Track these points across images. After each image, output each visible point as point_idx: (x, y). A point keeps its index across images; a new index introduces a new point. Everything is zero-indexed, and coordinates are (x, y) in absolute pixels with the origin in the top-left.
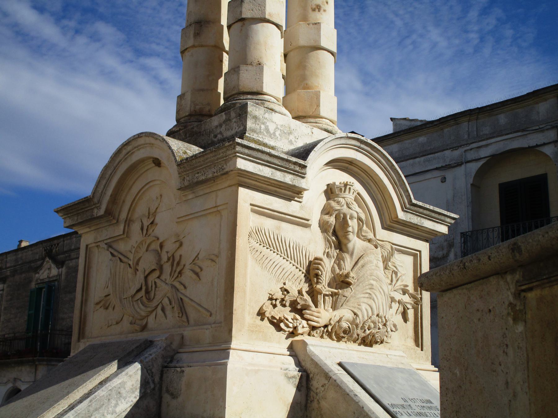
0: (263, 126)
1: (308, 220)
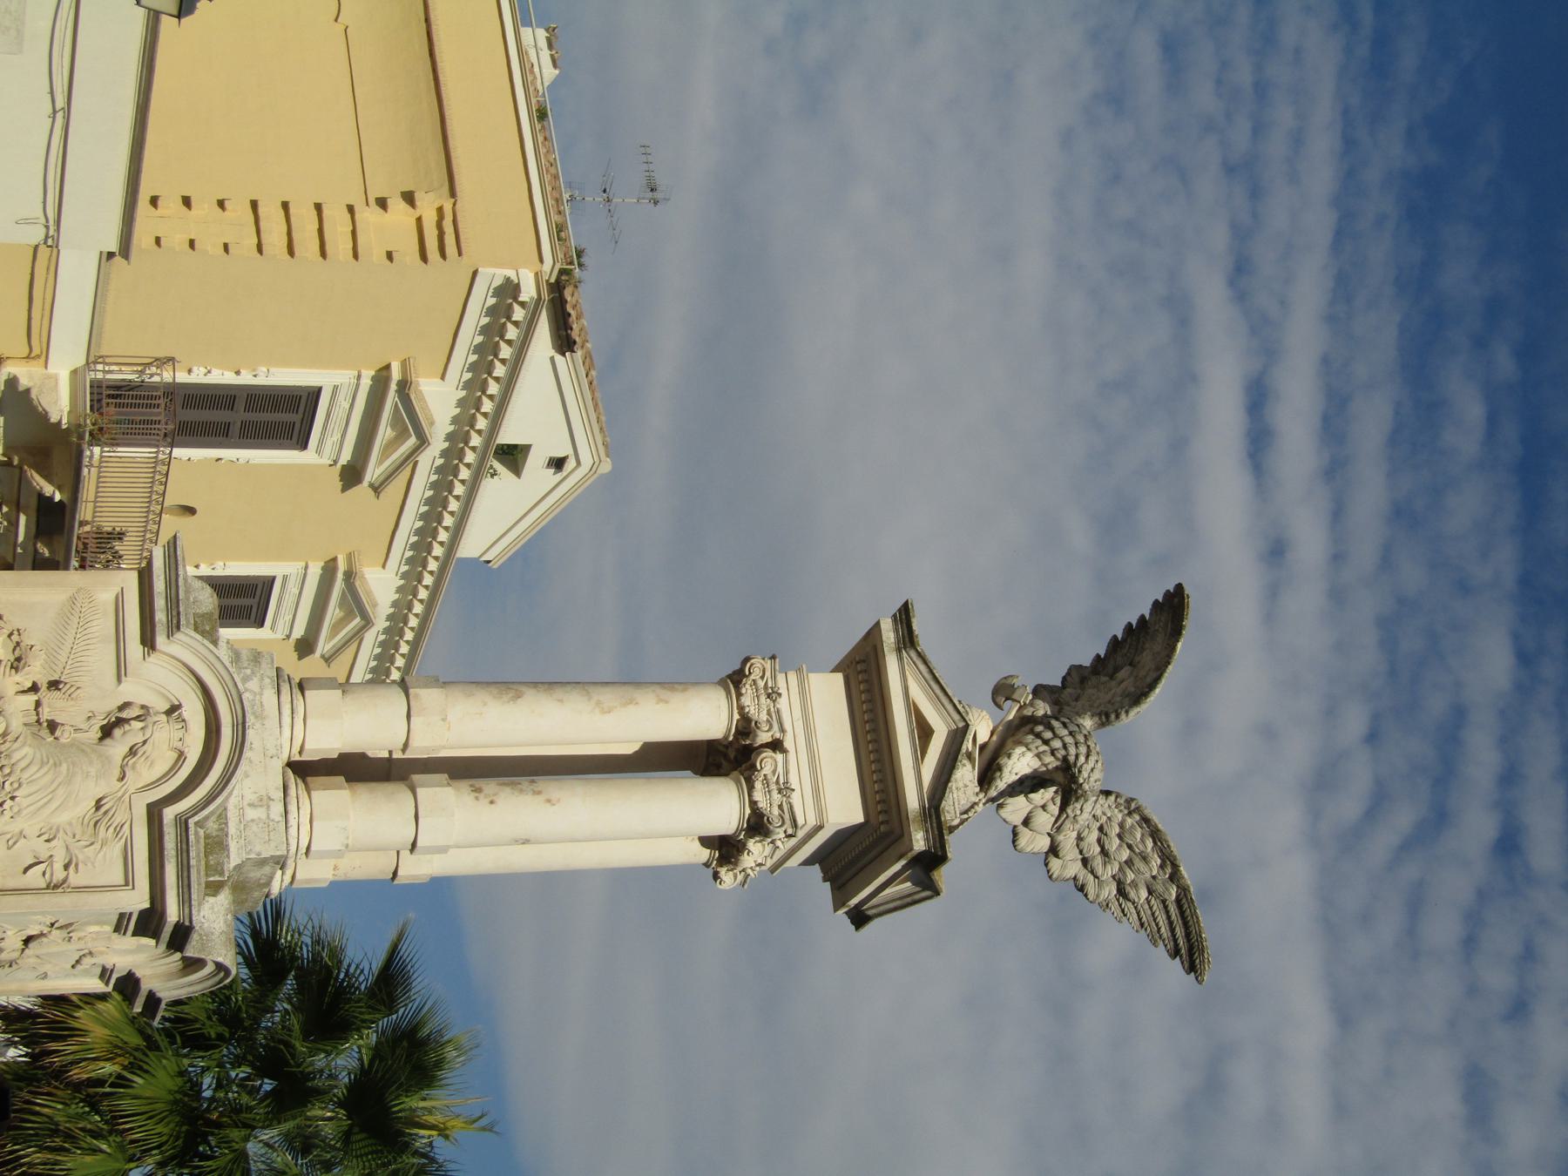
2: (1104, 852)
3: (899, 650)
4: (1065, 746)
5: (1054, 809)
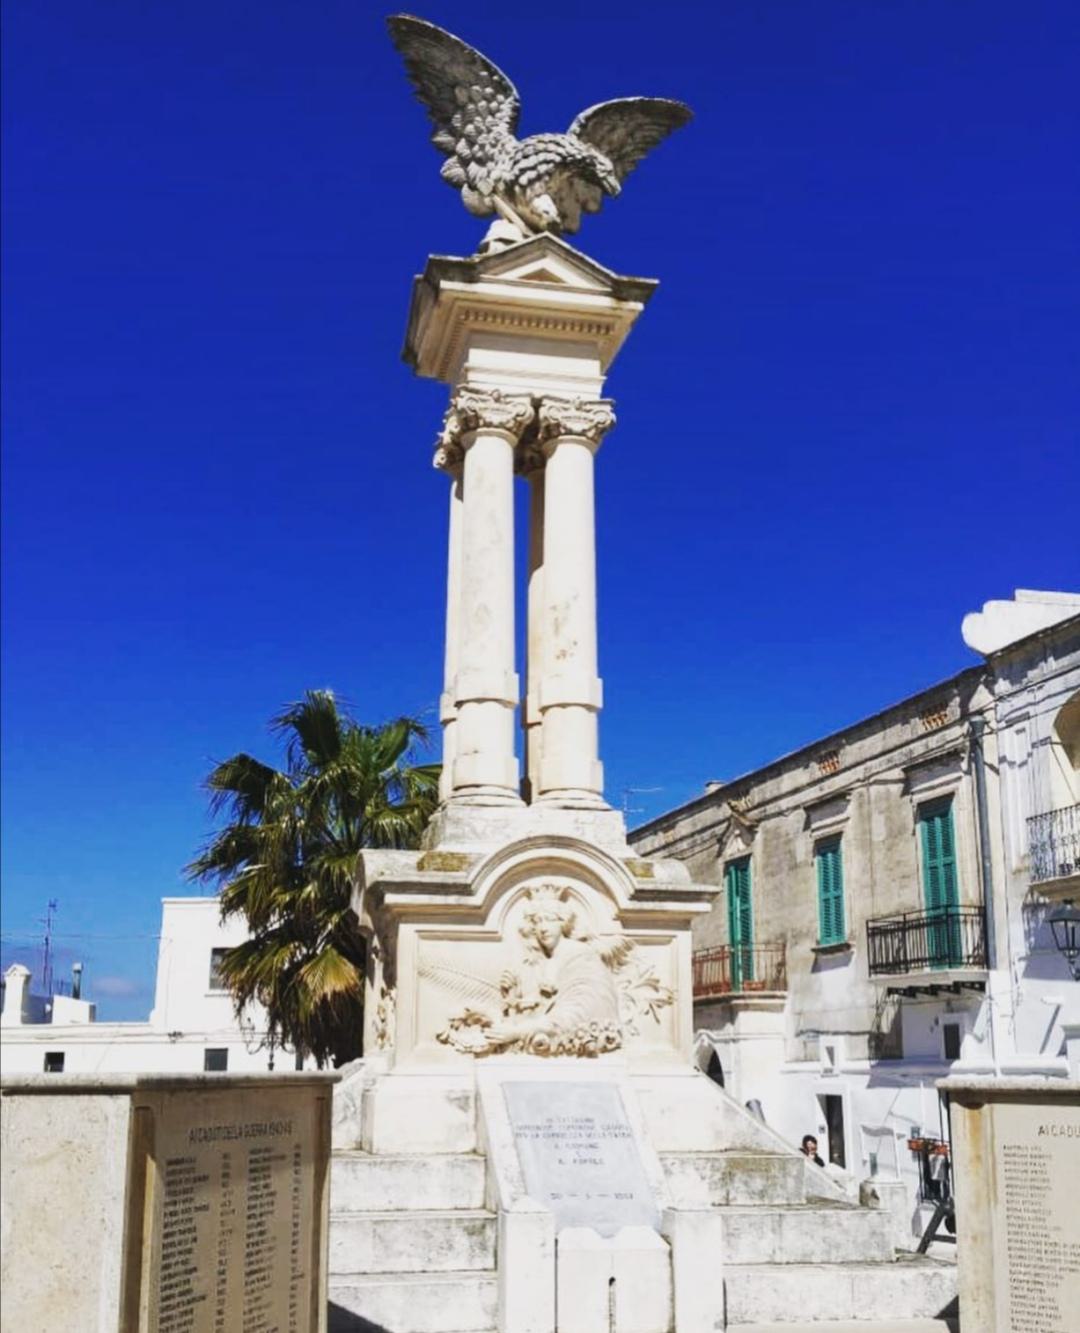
0: (467, 829)
1: (496, 932)
3: (472, 280)
4: (546, 162)
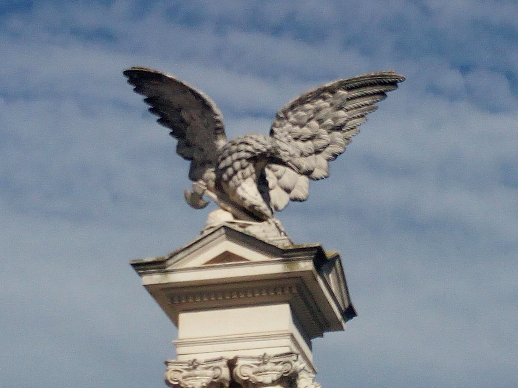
2: (312, 138)
4: (239, 159)
5: (281, 169)
